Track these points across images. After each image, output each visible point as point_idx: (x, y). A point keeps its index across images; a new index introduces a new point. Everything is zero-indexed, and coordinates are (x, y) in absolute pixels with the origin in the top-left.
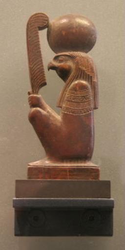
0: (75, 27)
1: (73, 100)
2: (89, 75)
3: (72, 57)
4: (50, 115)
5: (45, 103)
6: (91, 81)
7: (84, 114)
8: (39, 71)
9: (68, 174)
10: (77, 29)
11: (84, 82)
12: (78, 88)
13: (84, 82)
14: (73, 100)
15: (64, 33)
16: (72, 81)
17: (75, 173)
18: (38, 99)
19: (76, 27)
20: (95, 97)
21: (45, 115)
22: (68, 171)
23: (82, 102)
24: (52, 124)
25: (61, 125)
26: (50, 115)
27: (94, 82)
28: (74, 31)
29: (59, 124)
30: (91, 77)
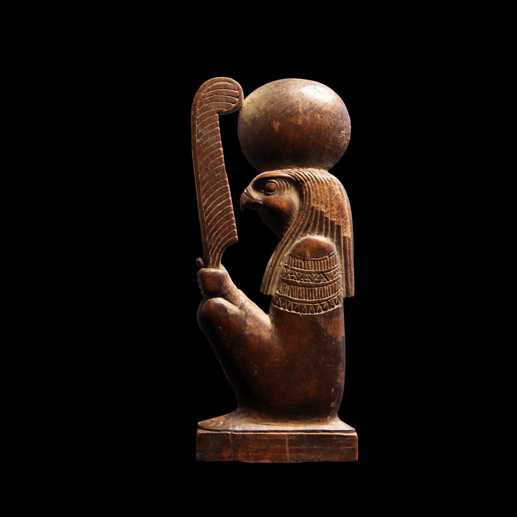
0: (301, 110)
1: (298, 282)
2: (332, 223)
3: (297, 184)
4: (246, 314)
5: (235, 287)
6: (339, 237)
7: (323, 312)
8: (221, 215)
9: (287, 449)
10: (308, 118)
11: (322, 239)
12: (308, 255)
13: (322, 239)
14: (298, 282)
15: (276, 125)
16: (295, 235)
17: (303, 447)
18: (220, 279)
19: (305, 112)
20: (346, 274)
21: (235, 316)
22: (287, 443)
23: (317, 286)
24: (251, 335)
25: (272, 336)
26: (246, 314)
27: (345, 238)
28: (300, 122)
29: (266, 335)
30: (339, 227)
